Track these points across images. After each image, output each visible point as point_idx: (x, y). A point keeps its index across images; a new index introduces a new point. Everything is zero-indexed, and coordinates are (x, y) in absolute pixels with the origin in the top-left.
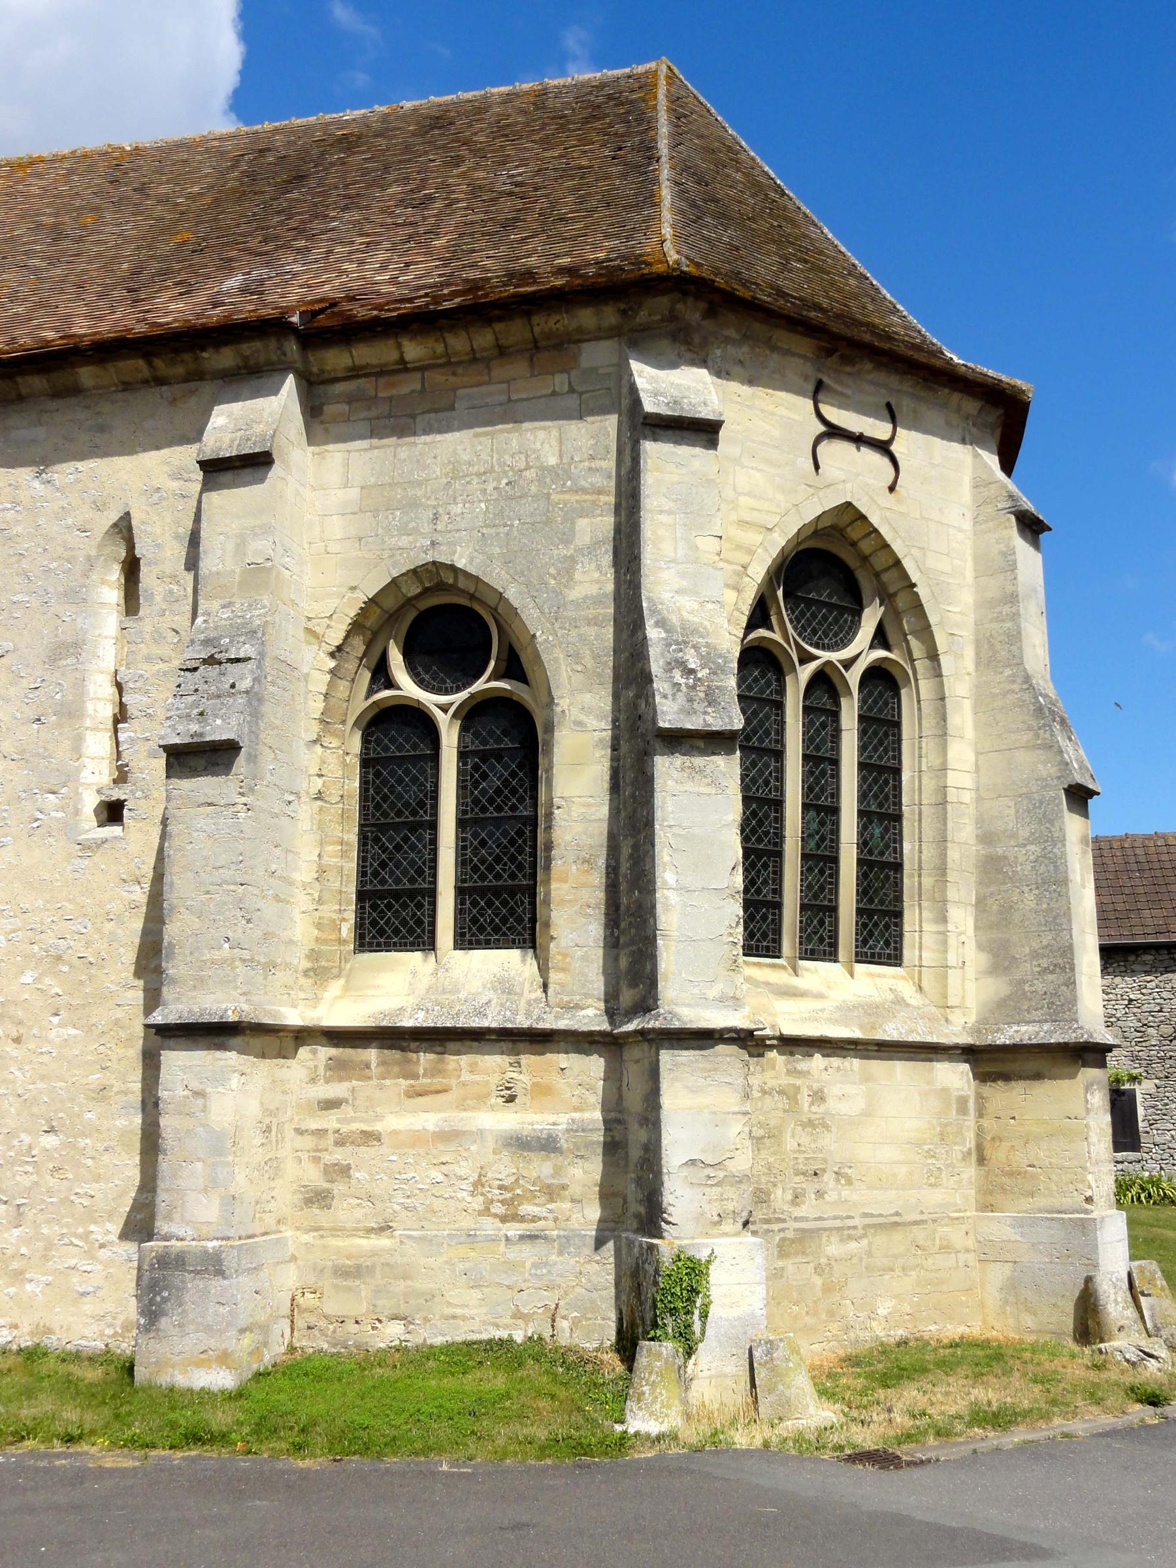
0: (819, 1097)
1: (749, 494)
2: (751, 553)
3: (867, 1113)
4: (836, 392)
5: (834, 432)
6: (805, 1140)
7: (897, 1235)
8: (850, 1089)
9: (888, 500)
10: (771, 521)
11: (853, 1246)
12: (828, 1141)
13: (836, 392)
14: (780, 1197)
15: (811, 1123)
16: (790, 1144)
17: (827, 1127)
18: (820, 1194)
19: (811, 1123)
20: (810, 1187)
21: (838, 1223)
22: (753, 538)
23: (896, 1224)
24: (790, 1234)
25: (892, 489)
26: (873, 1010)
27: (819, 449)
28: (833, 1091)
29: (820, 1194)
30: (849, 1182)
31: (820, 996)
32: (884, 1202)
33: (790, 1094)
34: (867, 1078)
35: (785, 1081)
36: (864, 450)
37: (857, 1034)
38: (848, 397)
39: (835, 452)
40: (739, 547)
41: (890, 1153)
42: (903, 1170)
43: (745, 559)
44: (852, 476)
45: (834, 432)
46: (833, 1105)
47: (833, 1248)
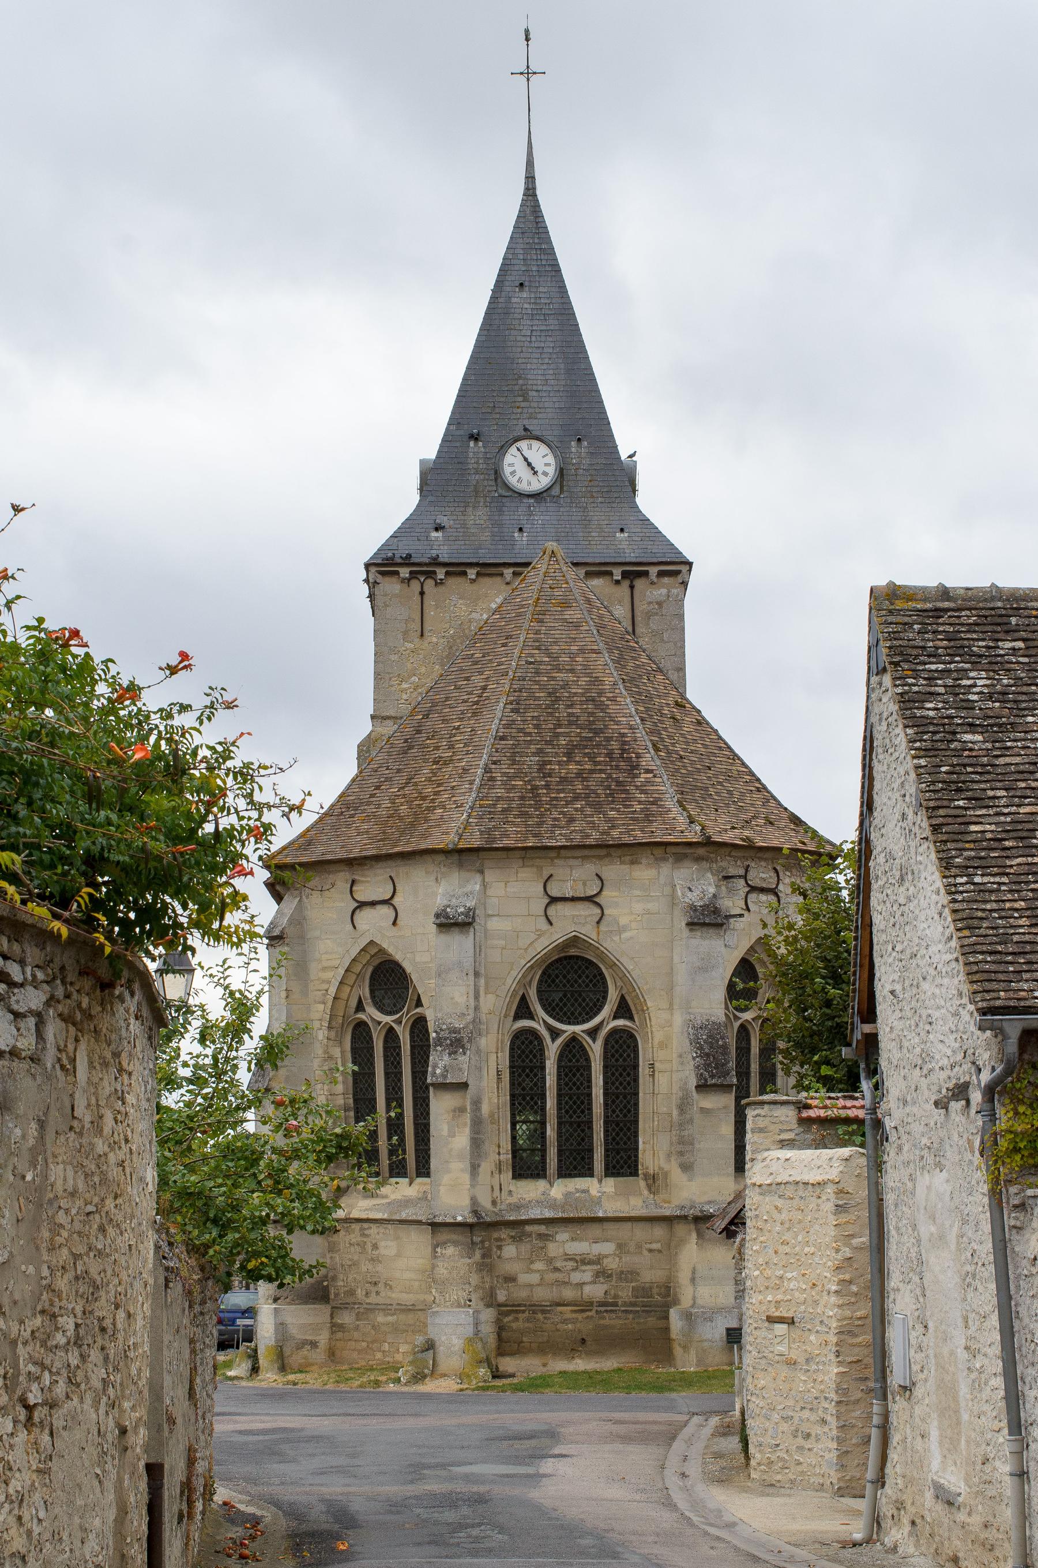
0: (375, 1247)
1: (326, 953)
2: (329, 982)
3: (398, 1255)
4: (363, 882)
5: (362, 905)
6: (370, 1267)
7: (411, 1316)
8: (389, 1243)
9: (393, 932)
10: (336, 963)
11: (390, 1319)
12: (379, 1268)
13: (363, 882)
14: (360, 1293)
15: (372, 1259)
16: (364, 1269)
17: (380, 1262)
18: (377, 1293)
19: (372, 1259)
20: (374, 1289)
21: (384, 1307)
22: (329, 975)
23: (410, 1310)
24: (362, 1310)
25: (394, 923)
26: (406, 1203)
27: (355, 918)
28: (382, 1244)
29: (377, 1293)
30: (391, 1288)
31: (386, 1197)
32: (407, 1298)
33: (362, 1245)
34: (397, 1238)
35: (359, 1239)
36: (378, 907)
37: (386, 1216)
38: (368, 882)
39: (360, 916)
40: (323, 981)
41: (408, 1275)
42: (417, 1283)
43: (325, 986)
44: (374, 924)
45: (362, 905)
46: (382, 1251)
47: (381, 1319)
